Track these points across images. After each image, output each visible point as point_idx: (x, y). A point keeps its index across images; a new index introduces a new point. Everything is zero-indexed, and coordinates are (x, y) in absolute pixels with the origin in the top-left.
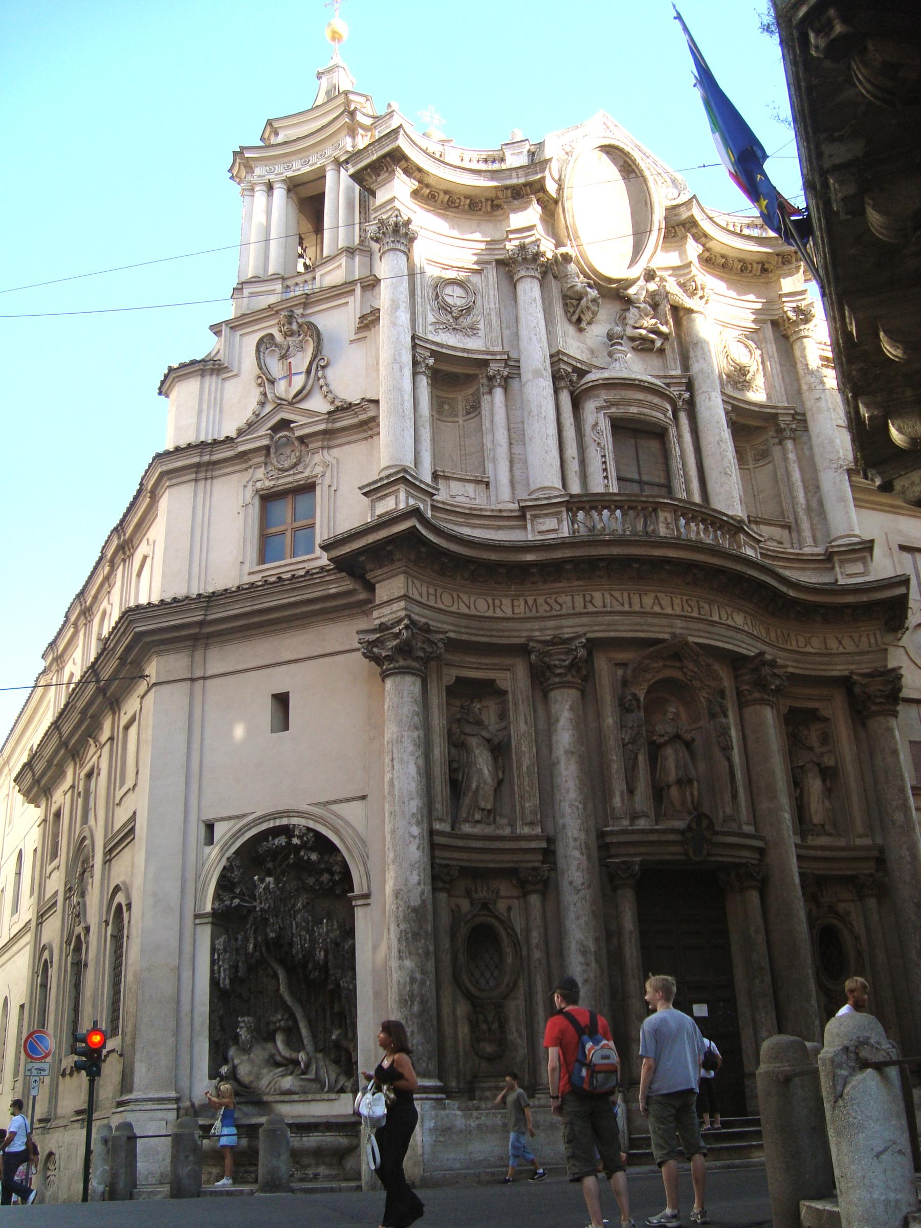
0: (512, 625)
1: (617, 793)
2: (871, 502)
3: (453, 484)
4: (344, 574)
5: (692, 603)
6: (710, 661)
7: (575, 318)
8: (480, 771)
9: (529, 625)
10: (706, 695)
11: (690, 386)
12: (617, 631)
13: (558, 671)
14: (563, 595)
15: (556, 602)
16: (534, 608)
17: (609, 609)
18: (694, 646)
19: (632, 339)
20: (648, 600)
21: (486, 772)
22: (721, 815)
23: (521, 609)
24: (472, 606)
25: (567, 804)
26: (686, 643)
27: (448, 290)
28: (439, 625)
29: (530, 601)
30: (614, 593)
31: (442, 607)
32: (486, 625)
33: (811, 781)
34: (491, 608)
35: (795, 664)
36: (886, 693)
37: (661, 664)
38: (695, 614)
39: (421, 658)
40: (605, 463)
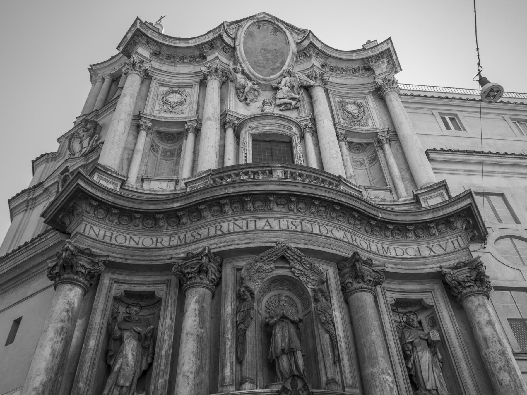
0: (166, 252)
1: (229, 365)
2: (449, 170)
3: (153, 183)
4: (57, 231)
5: (296, 224)
6: (311, 260)
7: (244, 98)
8: (126, 357)
9: (177, 251)
10: (312, 287)
11: (313, 120)
12: (235, 245)
13: (190, 276)
14: (203, 230)
15: (198, 234)
16: (184, 240)
17: (232, 232)
18: (296, 250)
19: (280, 105)
20: (261, 224)
21: (130, 357)
22: (324, 379)
23: (175, 241)
24: (140, 243)
25: (181, 375)
26: (288, 248)
27: (171, 96)
28: (98, 251)
29: (182, 236)
30: (237, 222)
31: (115, 243)
32: (147, 254)
33: (420, 353)
34: (155, 244)
35: (395, 266)
36: (472, 278)
37: (272, 266)
38: (299, 229)
39: (82, 273)
40: (246, 157)
